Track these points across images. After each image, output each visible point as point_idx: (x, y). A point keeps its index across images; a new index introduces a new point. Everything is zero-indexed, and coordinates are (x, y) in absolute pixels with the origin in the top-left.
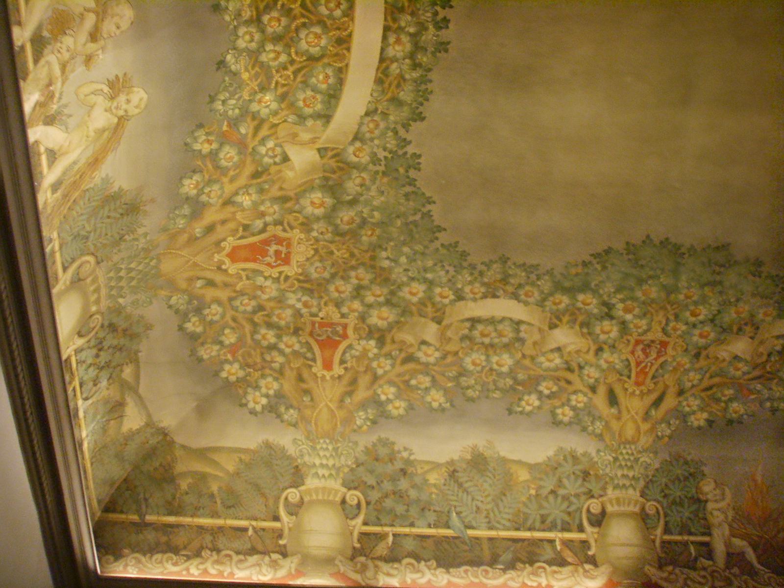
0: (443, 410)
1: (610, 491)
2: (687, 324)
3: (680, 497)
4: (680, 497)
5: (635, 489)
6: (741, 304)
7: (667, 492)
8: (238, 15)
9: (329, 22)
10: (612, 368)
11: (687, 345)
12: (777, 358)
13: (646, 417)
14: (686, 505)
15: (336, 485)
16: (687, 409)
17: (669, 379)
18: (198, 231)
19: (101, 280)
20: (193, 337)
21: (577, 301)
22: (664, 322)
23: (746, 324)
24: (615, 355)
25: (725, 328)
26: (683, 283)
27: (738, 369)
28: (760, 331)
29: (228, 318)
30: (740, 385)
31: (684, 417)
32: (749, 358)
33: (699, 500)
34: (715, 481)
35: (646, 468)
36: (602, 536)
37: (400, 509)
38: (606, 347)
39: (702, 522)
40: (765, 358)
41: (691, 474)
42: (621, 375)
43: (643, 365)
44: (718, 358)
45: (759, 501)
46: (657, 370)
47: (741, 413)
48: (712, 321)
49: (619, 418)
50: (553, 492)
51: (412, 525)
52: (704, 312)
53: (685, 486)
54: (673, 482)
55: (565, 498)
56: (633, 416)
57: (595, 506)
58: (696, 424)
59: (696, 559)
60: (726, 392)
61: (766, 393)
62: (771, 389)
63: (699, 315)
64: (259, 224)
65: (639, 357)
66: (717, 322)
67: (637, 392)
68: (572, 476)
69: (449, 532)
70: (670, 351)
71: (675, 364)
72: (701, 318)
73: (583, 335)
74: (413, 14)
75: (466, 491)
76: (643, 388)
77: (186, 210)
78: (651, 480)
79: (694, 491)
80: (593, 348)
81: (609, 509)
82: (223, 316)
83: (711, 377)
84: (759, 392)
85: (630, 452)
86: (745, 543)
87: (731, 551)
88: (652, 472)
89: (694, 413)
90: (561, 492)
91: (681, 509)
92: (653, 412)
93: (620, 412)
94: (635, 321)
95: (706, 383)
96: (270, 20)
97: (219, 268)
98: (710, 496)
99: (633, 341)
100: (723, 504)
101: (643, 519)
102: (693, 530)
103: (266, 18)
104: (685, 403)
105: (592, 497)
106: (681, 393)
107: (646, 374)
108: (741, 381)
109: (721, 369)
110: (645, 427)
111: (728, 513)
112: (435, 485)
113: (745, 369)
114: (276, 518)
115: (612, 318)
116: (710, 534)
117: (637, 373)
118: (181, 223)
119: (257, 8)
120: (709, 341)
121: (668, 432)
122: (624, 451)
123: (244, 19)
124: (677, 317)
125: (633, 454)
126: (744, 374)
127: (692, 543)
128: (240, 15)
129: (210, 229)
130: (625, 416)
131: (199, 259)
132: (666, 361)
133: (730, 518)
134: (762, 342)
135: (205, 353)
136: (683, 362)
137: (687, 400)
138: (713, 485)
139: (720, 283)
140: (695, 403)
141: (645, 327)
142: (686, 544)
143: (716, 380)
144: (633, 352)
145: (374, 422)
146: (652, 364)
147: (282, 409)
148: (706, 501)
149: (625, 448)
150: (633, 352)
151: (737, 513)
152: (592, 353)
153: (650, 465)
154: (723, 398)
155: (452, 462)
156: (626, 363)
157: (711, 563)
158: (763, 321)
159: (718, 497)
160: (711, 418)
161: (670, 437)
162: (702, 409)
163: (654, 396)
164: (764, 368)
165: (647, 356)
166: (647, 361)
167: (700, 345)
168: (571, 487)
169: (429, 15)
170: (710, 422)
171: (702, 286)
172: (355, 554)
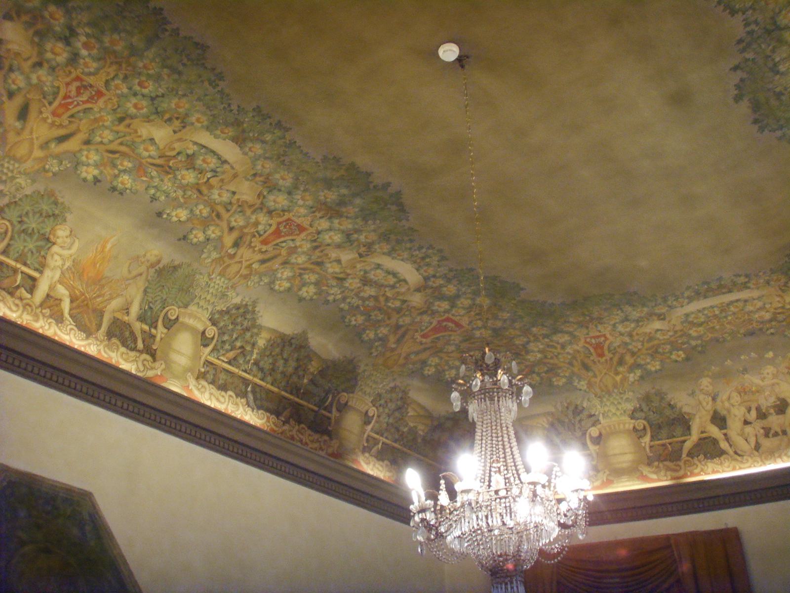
2: (130, 89)
3: (33, 229)
4: (33, 229)
6: (184, 100)
7: (25, 219)
10: (39, 87)
11: (119, 106)
12: (183, 160)
13: (45, 146)
14: (35, 237)
16: (84, 159)
17: (84, 125)
21: (47, 10)
22: (112, 76)
23: (177, 118)
24: (50, 78)
25: (159, 111)
26: (150, 53)
27: (146, 150)
28: (184, 131)
30: (141, 165)
31: (77, 164)
32: (161, 147)
33: (48, 240)
34: (71, 232)
35: (17, 189)
38: (46, 65)
39: (41, 259)
40: (173, 153)
41: (54, 215)
42: (44, 98)
43: (70, 100)
44: (136, 132)
45: (98, 266)
46: (79, 112)
47: (127, 186)
48: (153, 99)
49: (18, 134)
52: (150, 88)
53: (43, 222)
54: (34, 213)
56: (32, 139)
58: (84, 175)
59: (18, 287)
60: (126, 163)
61: (156, 182)
62: (162, 180)
63: (145, 88)
65: (70, 92)
66: (155, 102)
67: (49, 121)
70: (101, 103)
71: (98, 115)
72: (145, 91)
73: (32, 42)
76: (57, 119)
78: (15, 202)
79: (48, 230)
80: (35, 59)
83: (121, 144)
84: (152, 178)
85: (11, 167)
86: (66, 293)
87: (52, 294)
88: (21, 196)
89: (88, 165)
91: (28, 239)
92: (53, 145)
93: (23, 129)
94: (87, 60)
95: (113, 147)
98: (59, 241)
99: (73, 75)
100: (66, 253)
102: (28, 262)
104: (85, 153)
106: (87, 142)
107: (68, 109)
108: (144, 161)
109: (134, 142)
110: (38, 153)
111: (66, 263)
113: (153, 153)
115: (68, 44)
116: (41, 272)
117: (61, 105)
120: (138, 114)
121: (56, 169)
122: (6, 165)
124: (126, 78)
125: (12, 171)
126: (150, 157)
127: (22, 272)
130: (26, 135)
132: (91, 109)
133: (65, 267)
134: (180, 140)
136: (106, 118)
137: (89, 151)
138: (68, 233)
139: (180, 73)
140: (94, 157)
141: (92, 70)
142: (15, 271)
143: (123, 149)
144: (68, 84)
146: (78, 104)
148: (54, 244)
149: (8, 162)
150: (68, 84)
151: (73, 266)
152: (30, 63)
153: (23, 188)
154: (120, 167)
156: (55, 90)
157: (29, 296)
158: (193, 124)
159: (66, 245)
160: (99, 177)
161: (55, 174)
162: (96, 166)
163: (62, 132)
164: (169, 161)
165: (79, 93)
166: (75, 99)
167: (130, 112)
170: (96, 180)
171: (164, 66)
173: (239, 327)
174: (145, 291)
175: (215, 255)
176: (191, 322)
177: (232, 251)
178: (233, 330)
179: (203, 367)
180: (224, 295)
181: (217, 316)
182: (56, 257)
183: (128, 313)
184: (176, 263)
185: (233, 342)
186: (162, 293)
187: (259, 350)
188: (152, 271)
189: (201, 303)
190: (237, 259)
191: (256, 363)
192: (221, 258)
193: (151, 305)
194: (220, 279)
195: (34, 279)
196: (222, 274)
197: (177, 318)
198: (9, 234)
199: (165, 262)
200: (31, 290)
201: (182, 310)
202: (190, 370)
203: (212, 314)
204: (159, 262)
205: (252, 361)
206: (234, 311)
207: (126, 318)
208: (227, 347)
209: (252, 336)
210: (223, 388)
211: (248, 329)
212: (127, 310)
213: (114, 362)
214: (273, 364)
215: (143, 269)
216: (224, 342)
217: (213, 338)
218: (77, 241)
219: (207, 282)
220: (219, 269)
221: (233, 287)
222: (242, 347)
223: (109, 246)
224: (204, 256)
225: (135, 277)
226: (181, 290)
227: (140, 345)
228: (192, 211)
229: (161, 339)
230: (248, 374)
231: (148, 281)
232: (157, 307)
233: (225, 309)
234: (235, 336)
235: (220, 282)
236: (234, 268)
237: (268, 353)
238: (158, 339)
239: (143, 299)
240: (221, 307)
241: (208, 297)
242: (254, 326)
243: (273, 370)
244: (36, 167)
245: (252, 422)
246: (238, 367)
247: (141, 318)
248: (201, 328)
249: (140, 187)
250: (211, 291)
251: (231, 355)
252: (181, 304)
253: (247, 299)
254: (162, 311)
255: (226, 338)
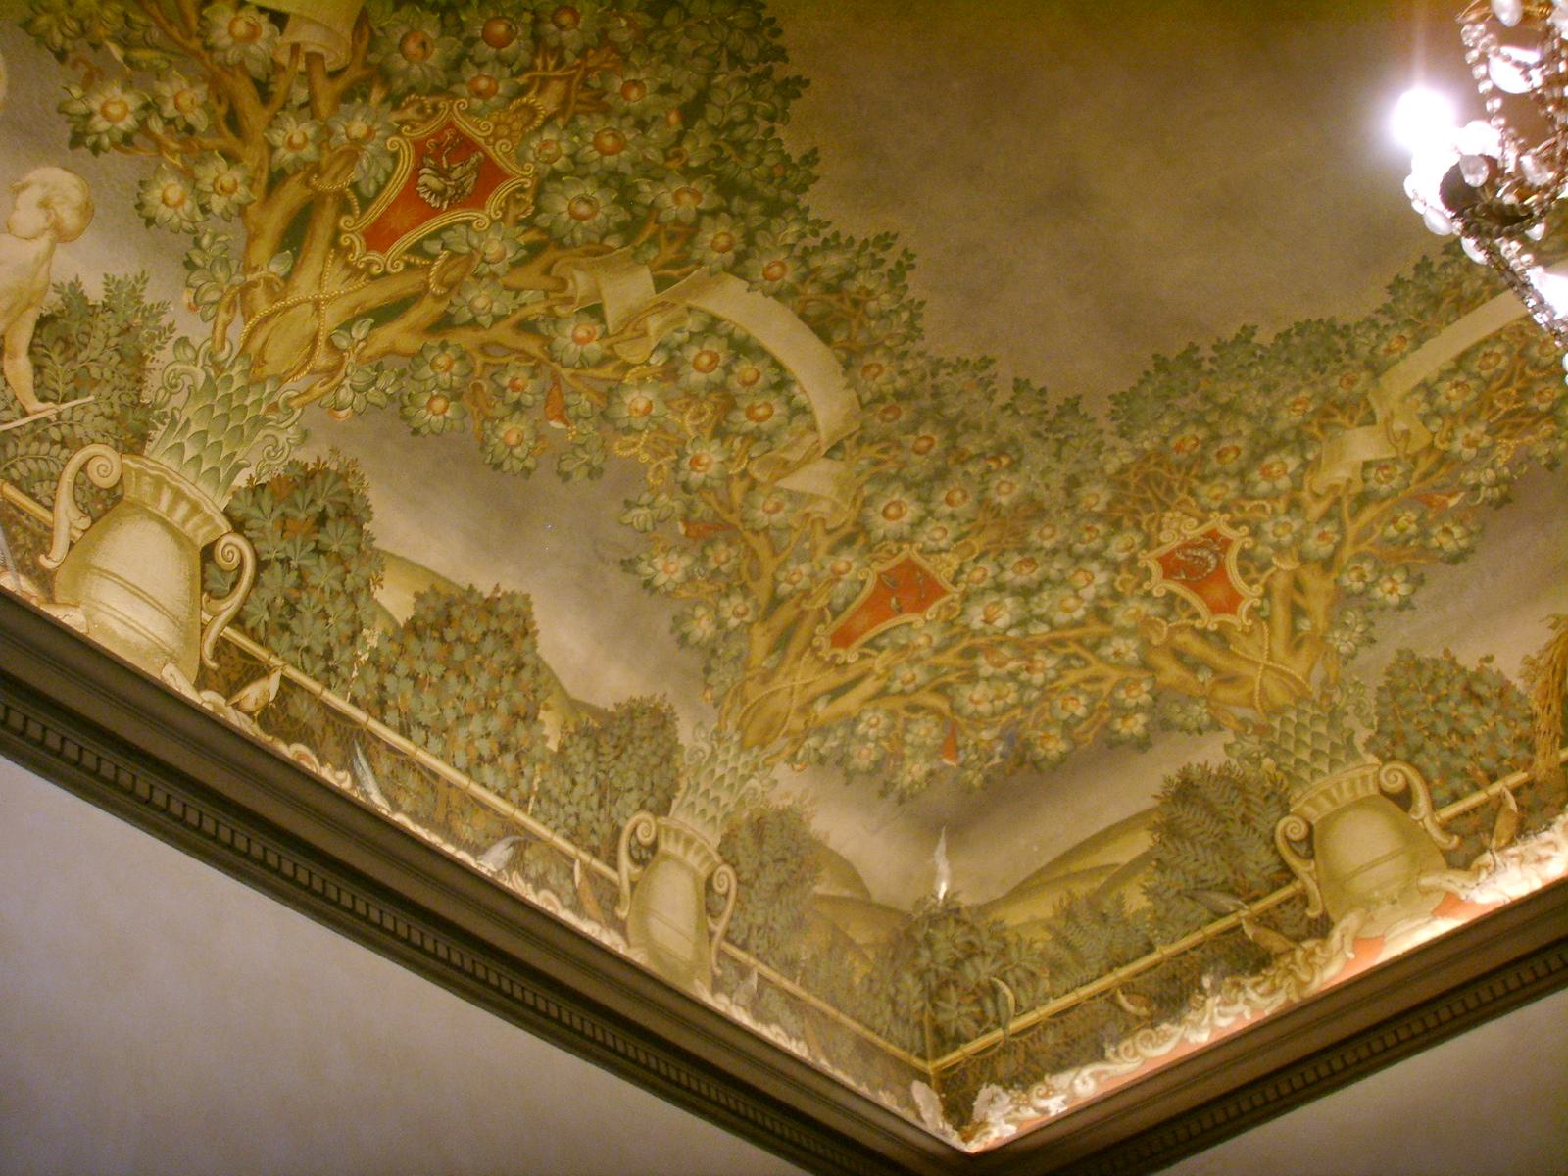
8: (1554, 437)
9: (1517, 347)
74: (1458, 285)
96: (1541, 401)
103: (1543, 407)
119: (1535, 423)
123: (1555, 428)
128: (1553, 436)
169: (1450, 271)
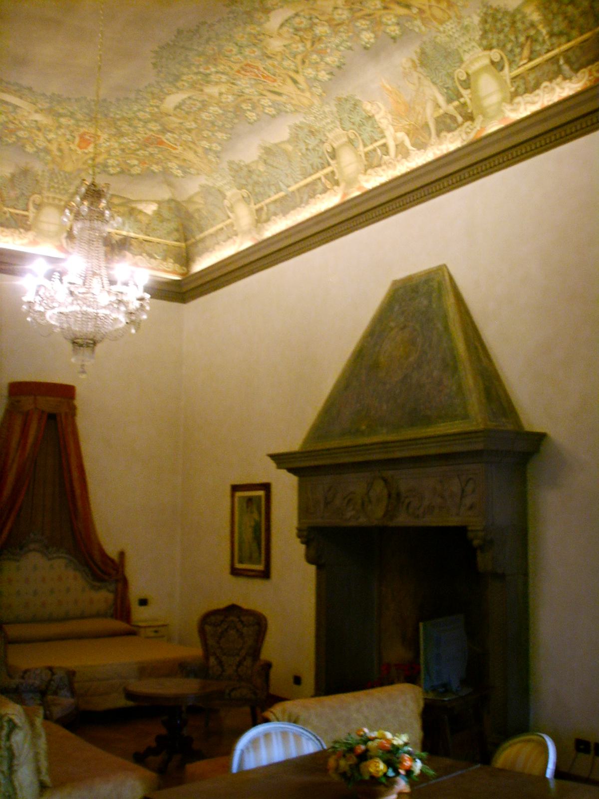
0: (230, 138)
1: (328, 134)
5: (338, 128)
14: (365, 123)
15: (235, 190)
18: (58, 154)
19: (51, 195)
20: (122, 172)
29: (120, 159)
35: (332, 114)
36: (338, 163)
37: (261, 190)
39: (378, 130)
50: (307, 149)
51: (269, 196)
55: (314, 150)
57: (327, 147)
64: (68, 137)
68: (308, 137)
69: (282, 194)
75: (277, 168)
77: (42, 154)
79: (364, 113)
81: (335, 146)
82: (117, 160)
87: (398, 143)
90: (310, 147)
91: (364, 127)
93: (288, 96)
97: (86, 154)
98: (373, 112)
100: (382, 113)
101: (351, 143)
105: (324, 143)
112: (265, 172)
114: (229, 217)
116: (384, 137)
118: (49, 158)
129: (60, 150)
131: (74, 157)
133: (390, 119)
135: (136, 170)
142: (375, 150)
145: (218, 157)
147: (187, 170)
155: (260, 158)
168: (312, 142)
172: (258, 221)
173: (506, 29)
174: (434, 83)
175: (418, 22)
176: (477, 66)
177: (415, 11)
178: (506, 36)
179: (513, 86)
180: (466, 29)
181: (485, 42)
182: (382, 121)
183: (440, 107)
184: (419, 50)
185: (517, 43)
186: (441, 72)
187: (541, 23)
188: (419, 69)
189: (466, 48)
190: (426, 8)
191: (552, 35)
192: (423, 19)
193: (446, 86)
194: (447, 25)
195: (384, 145)
196: (442, 22)
197: (468, 74)
198: (357, 135)
199: (415, 58)
200: (387, 153)
201: (464, 66)
202: (504, 100)
203: (480, 45)
204: (413, 61)
205: (547, 37)
206: (487, 26)
207: (441, 111)
208: (517, 50)
209: (523, 23)
210: (537, 86)
211: (514, 23)
212: (438, 106)
213: (445, 152)
214: (566, 18)
215: (416, 75)
216: (512, 51)
217: (502, 58)
218: (378, 103)
219: (447, 36)
220: (436, 24)
221: (460, 18)
222: (527, 38)
223: (388, 86)
224: (417, 30)
225: (420, 83)
226: (446, 57)
227: (460, 119)
228: (363, 30)
229: (471, 99)
230: (553, 50)
231: (428, 76)
232: (449, 84)
233: (481, 33)
234: (512, 37)
235: (450, 26)
236: (438, 13)
237: (550, 16)
238: (468, 101)
239: (438, 88)
240: (477, 35)
241: (462, 40)
242: (513, 15)
243: (571, 22)
244: (318, 99)
245: (571, 93)
246: (539, 55)
247: (449, 101)
248: (486, 61)
249: (338, 54)
250: (456, 35)
251: (526, 52)
252: (458, 64)
253: (479, 11)
254: (455, 82)
255: (509, 46)
